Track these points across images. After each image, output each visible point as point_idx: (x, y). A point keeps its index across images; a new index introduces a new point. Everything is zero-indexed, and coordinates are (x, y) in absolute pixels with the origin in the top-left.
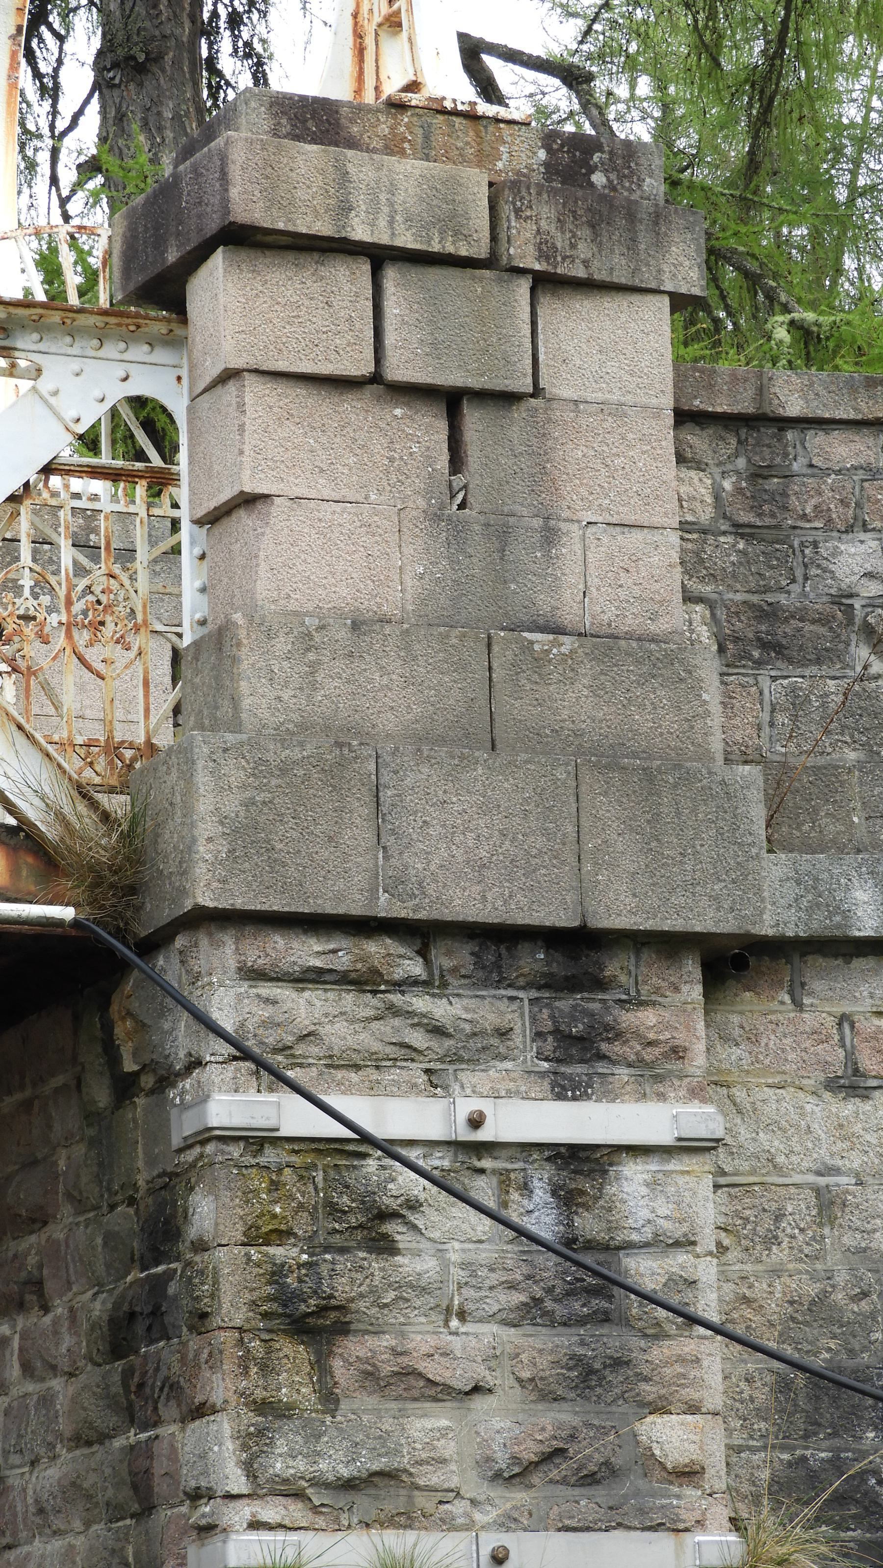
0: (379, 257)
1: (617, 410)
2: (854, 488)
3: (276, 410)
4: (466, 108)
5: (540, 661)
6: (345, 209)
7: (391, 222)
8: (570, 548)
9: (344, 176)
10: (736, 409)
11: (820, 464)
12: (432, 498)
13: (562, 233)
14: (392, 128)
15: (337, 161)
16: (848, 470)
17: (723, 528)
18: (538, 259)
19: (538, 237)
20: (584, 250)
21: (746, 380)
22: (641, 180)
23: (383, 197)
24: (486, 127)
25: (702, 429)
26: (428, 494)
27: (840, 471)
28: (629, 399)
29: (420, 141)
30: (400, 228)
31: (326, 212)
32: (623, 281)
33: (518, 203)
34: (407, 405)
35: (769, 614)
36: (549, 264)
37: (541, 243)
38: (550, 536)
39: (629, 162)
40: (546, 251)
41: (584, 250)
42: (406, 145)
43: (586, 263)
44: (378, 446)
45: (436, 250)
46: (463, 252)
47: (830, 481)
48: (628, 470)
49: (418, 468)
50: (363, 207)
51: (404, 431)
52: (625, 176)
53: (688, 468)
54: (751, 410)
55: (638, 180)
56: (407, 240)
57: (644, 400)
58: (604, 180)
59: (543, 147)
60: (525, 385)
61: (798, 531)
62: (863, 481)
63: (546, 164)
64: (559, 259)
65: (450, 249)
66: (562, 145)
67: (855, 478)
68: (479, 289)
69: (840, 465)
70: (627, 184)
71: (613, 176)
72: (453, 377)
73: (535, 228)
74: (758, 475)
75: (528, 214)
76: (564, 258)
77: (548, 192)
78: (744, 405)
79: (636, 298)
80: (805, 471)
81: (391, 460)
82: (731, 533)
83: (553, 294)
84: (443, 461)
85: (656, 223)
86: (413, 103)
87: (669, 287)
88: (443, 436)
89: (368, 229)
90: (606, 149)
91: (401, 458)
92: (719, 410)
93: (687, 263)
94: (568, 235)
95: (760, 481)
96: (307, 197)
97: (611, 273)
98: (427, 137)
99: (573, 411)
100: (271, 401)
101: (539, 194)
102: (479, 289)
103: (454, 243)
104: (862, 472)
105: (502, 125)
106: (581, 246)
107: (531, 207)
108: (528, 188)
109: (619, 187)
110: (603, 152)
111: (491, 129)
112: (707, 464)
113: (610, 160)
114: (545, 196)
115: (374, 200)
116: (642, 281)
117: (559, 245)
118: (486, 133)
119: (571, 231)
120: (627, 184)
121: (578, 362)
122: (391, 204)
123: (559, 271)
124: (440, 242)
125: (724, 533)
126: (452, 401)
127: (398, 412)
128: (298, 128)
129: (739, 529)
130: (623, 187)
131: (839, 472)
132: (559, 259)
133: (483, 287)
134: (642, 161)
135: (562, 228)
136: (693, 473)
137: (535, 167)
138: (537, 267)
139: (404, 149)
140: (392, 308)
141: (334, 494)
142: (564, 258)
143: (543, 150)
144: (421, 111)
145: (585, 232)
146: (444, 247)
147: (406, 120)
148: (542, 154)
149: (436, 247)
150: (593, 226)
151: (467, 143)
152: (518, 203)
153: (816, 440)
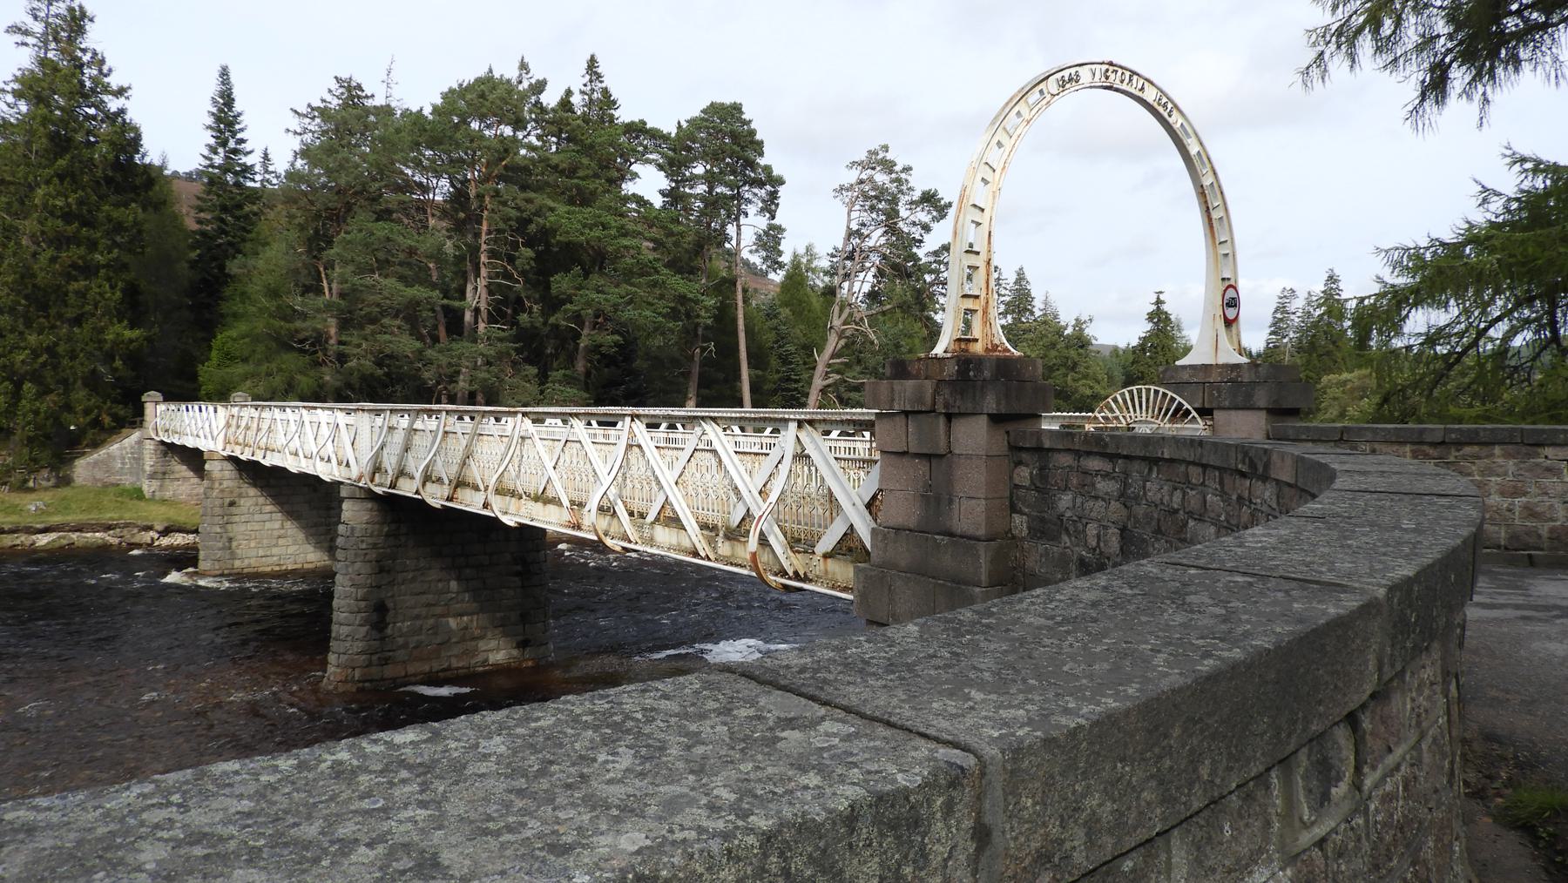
0: (906, 413)
1: (969, 457)
5: (938, 546)
8: (955, 506)
35: (1042, 520)
38: (951, 502)
40: (946, 406)
56: (908, 408)
60: (942, 452)
72: (925, 451)
74: (1041, 469)
126: (928, 457)
129: (1037, 489)
153: (1056, 456)
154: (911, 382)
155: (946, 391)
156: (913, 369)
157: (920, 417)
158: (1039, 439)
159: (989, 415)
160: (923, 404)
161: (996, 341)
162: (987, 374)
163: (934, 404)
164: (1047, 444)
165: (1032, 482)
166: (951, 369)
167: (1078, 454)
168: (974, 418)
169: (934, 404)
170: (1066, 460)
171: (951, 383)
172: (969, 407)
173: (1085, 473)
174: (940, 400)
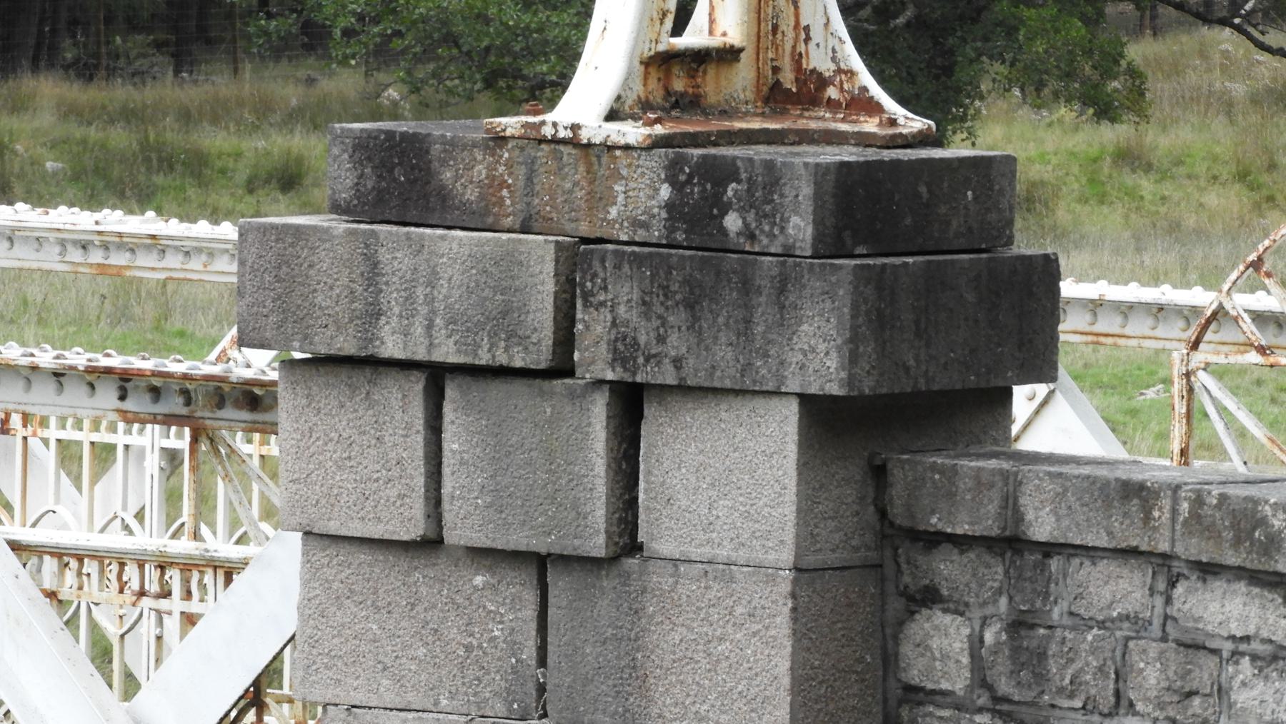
2: (1114, 651)
3: (336, 585)
4: (569, 134)
6: (374, 314)
7: (429, 327)
9: (373, 271)
10: (978, 530)
11: (1082, 611)
12: (514, 701)
13: (649, 320)
14: (491, 168)
15: (367, 246)
16: (1113, 620)
17: (980, 702)
18: (612, 365)
19: (614, 331)
20: (676, 344)
21: (992, 486)
22: (785, 220)
23: (420, 292)
24: (599, 157)
25: (962, 552)
26: (508, 695)
27: (1103, 622)
28: (742, 555)
29: (521, 183)
30: (440, 334)
31: (351, 321)
32: (728, 384)
33: (589, 284)
34: (490, 569)
36: (626, 369)
37: (616, 340)
39: (771, 193)
40: (624, 349)
41: (676, 344)
42: (505, 192)
43: (678, 363)
44: (452, 633)
45: (483, 362)
46: (518, 363)
47: (1090, 638)
48: (733, 660)
49: (499, 659)
50: (396, 310)
51: (485, 607)
52: (766, 216)
53: (945, 611)
54: (995, 532)
55: (782, 219)
56: (447, 353)
57: (759, 556)
58: (740, 222)
59: (667, 180)
60: (597, 545)
61: (1057, 713)
62: (1128, 639)
63: (669, 206)
64: (641, 360)
65: (502, 359)
66: (691, 176)
67: (1118, 634)
68: (549, 410)
69: (1105, 612)
70: (767, 228)
71: (751, 216)
73: (609, 318)
74: (1019, 625)
75: (602, 298)
76: (647, 360)
77: (630, 263)
78: (988, 525)
79: (759, 402)
80: (1067, 621)
81: (469, 648)
82: (988, 710)
83: (660, 403)
84: (529, 653)
85: (782, 290)
86: (508, 133)
87: (793, 385)
88: (530, 613)
89: (399, 338)
90: (744, 176)
91: (480, 646)
92: (959, 531)
93: (822, 347)
94: (657, 323)
95: (1023, 633)
96: (329, 302)
97: (712, 375)
98: (529, 179)
99: (672, 576)
100: (329, 573)
101: (618, 267)
102: (549, 410)
103: (506, 349)
104: (1126, 625)
105: (618, 153)
106: (673, 338)
107: (605, 289)
108: (603, 261)
109: (757, 232)
110: (739, 182)
111: (605, 159)
112: (967, 605)
113: (749, 190)
114: (626, 268)
115: (410, 299)
116: (754, 382)
117: (642, 339)
118: (600, 164)
119: (660, 317)
120: (767, 228)
121: (684, 503)
122: (429, 300)
123: (639, 379)
124: (489, 351)
125: (980, 710)
126: (540, 565)
127: (479, 580)
128: (384, 179)
130: (762, 231)
131: (1101, 625)
132: (641, 360)
133: (553, 407)
134: (787, 190)
135: (646, 315)
136: (948, 619)
137: (656, 211)
138: (610, 376)
139: (502, 198)
140: (452, 444)
141: (398, 699)
142: (647, 360)
143: (666, 185)
144: (520, 142)
145: (678, 318)
146: (494, 357)
147: (506, 155)
148: (665, 192)
149: (484, 359)
150: (691, 305)
151: (576, 184)
152: (589, 284)
154: (454, 245)
155: (624, 293)
156: (465, 179)
157: (497, 390)
158: (1011, 508)
159: (806, 401)
160: (514, 337)
161: (819, 61)
162: (800, 228)
163: (565, 338)
164: (1042, 527)
165: (981, 680)
166: (641, 197)
167: (1166, 569)
168: (744, 409)
169: (565, 338)
170: (1117, 590)
171: (645, 258)
172: (724, 360)
173: (1194, 646)
174: (593, 329)
